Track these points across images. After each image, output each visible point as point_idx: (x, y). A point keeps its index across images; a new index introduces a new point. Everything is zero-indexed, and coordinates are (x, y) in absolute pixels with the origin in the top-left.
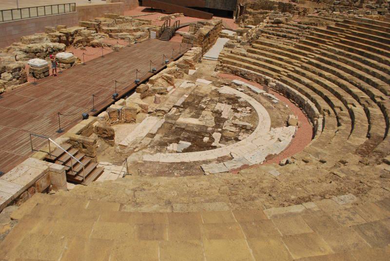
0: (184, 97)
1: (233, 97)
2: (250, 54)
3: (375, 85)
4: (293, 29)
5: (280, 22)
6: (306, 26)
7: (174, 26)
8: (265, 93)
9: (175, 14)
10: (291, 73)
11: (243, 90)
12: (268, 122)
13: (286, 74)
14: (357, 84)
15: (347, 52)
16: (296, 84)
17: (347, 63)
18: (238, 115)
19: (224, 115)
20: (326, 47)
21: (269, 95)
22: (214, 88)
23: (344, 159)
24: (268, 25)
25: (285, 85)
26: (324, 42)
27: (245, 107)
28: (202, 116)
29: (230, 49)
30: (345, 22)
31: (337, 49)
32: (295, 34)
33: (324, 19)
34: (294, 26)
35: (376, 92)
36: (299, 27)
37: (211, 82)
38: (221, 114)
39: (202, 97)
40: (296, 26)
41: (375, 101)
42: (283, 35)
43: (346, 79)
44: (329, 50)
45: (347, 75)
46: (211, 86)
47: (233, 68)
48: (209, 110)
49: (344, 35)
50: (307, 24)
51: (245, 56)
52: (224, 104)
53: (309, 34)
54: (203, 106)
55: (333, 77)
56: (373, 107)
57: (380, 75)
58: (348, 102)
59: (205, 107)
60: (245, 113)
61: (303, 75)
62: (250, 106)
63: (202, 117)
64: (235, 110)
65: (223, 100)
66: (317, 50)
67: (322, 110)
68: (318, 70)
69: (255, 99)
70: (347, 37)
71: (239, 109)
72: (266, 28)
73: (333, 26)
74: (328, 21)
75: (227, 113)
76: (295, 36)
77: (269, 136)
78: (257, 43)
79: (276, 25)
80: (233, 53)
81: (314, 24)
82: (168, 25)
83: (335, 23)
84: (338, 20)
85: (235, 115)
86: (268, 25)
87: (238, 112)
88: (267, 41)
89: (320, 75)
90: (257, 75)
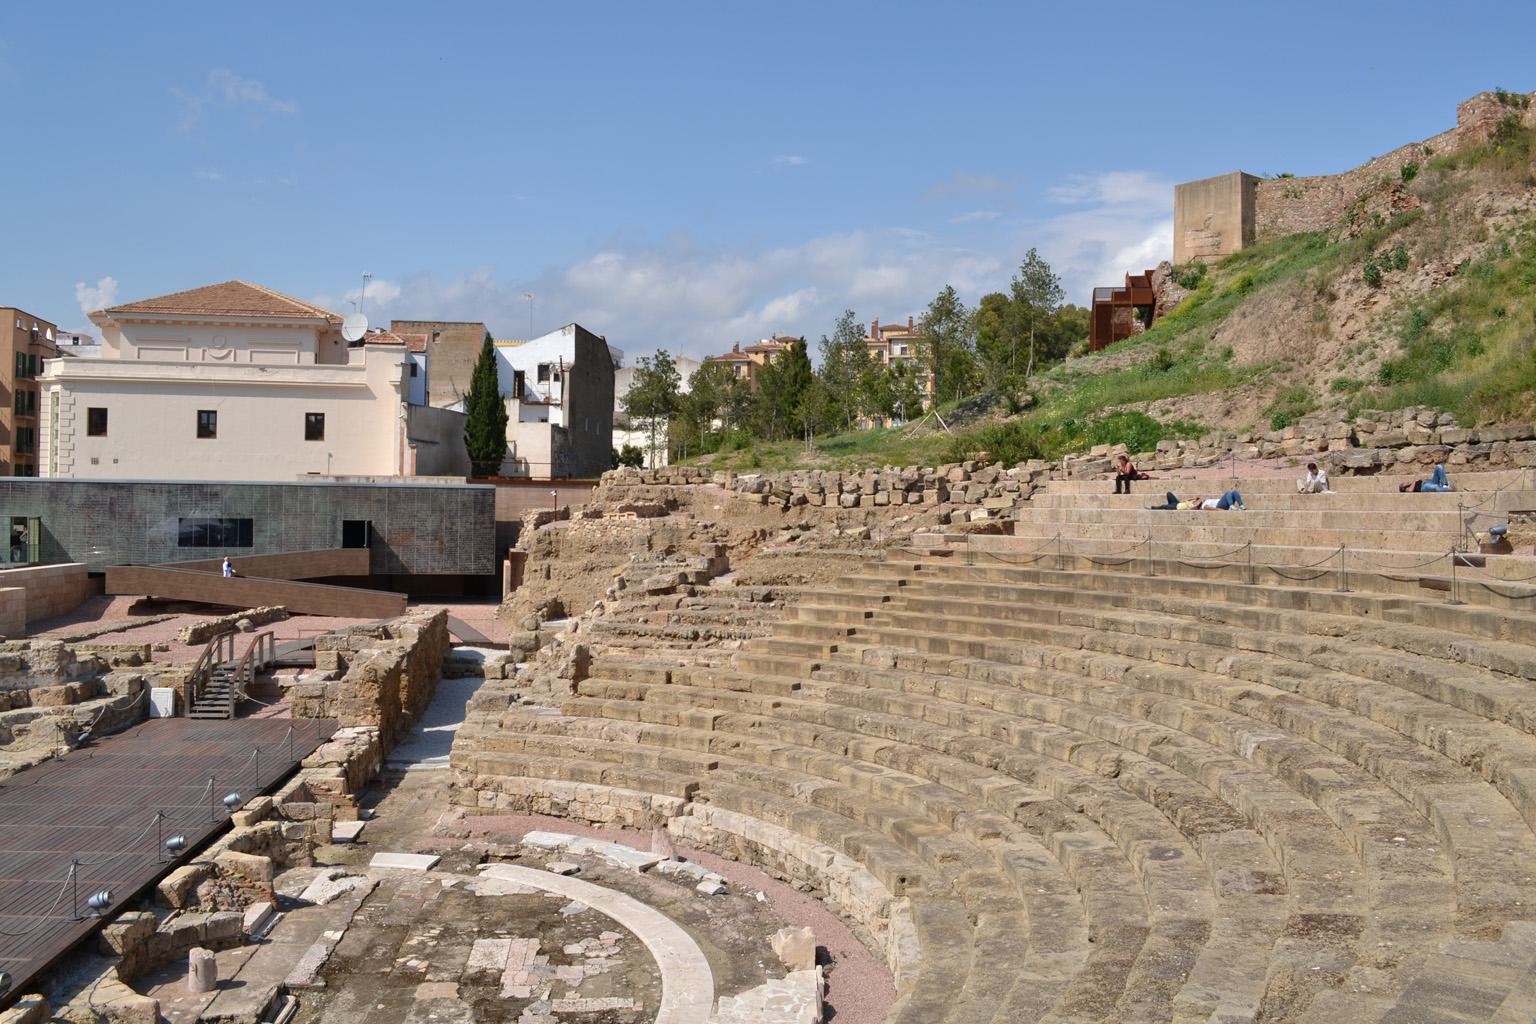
0: (327, 941)
1: (534, 903)
2: (580, 722)
7: (251, 653)
9: (251, 612)
11: (574, 867)
12: (704, 977)
18: (571, 974)
19: (513, 987)
22: (448, 881)
27: (596, 934)
28: (415, 1007)
37: (433, 858)
38: (497, 982)
39: (406, 930)
46: (435, 874)
48: (445, 975)
49: (902, 600)
52: (506, 941)
54: (413, 963)
56: (1071, 829)
59: (422, 966)
60: (597, 957)
62: (614, 925)
63: (418, 1013)
64: (559, 958)
65: (498, 924)
69: (628, 893)
71: (572, 949)
75: (523, 976)
82: (225, 658)
87: (568, 960)
90: (620, 797)
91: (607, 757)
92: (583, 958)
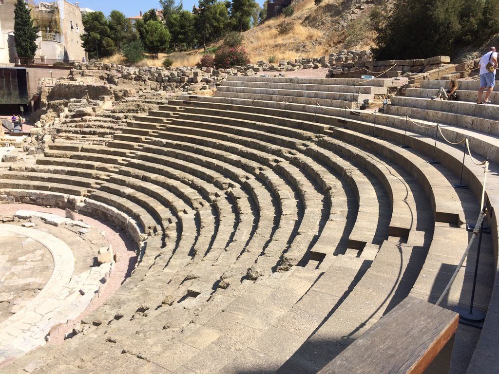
2: (42, 167)
3: (209, 179)
4: (105, 121)
5: (86, 114)
6: (121, 115)
8: (69, 221)
10: (106, 184)
13: (99, 186)
14: (191, 182)
15: (175, 142)
16: (115, 198)
17: (177, 156)
18: (18, 268)
20: (150, 139)
21: (74, 222)
23: (144, 305)
24: (68, 120)
25: (99, 203)
26: (146, 134)
29: (8, 164)
30: (170, 103)
31: (164, 141)
32: (108, 128)
33: (146, 102)
34: (106, 116)
35: (210, 188)
36: (113, 117)
40: (109, 116)
41: (209, 200)
42: (90, 132)
43: (177, 179)
44: (154, 143)
45: (177, 173)
47: (17, 192)
50: (123, 112)
51: (33, 170)
53: (126, 124)
55: (161, 178)
57: (214, 164)
58: (178, 209)
60: (30, 261)
61: (122, 183)
64: (14, 261)
66: (139, 146)
67: (147, 229)
68: (142, 173)
70: (174, 123)
71: (21, 259)
72: (65, 125)
73: (156, 110)
74: (150, 104)
76: (108, 131)
77: (67, 290)
78: (51, 148)
79: (79, 119)
80: (14, 170)
81: (133, 110)
83: (158, 106)
84: (164, 101)
85: (11, 271)
86: (68, 120)
88: (68, 143)
89: (145, 179)
90: (56, 196)
91: (53, 180)
92: (26, 261)
